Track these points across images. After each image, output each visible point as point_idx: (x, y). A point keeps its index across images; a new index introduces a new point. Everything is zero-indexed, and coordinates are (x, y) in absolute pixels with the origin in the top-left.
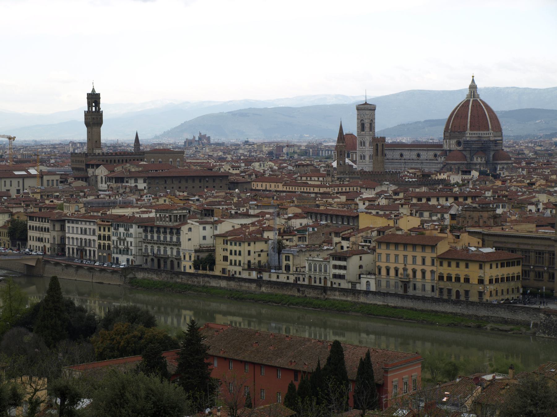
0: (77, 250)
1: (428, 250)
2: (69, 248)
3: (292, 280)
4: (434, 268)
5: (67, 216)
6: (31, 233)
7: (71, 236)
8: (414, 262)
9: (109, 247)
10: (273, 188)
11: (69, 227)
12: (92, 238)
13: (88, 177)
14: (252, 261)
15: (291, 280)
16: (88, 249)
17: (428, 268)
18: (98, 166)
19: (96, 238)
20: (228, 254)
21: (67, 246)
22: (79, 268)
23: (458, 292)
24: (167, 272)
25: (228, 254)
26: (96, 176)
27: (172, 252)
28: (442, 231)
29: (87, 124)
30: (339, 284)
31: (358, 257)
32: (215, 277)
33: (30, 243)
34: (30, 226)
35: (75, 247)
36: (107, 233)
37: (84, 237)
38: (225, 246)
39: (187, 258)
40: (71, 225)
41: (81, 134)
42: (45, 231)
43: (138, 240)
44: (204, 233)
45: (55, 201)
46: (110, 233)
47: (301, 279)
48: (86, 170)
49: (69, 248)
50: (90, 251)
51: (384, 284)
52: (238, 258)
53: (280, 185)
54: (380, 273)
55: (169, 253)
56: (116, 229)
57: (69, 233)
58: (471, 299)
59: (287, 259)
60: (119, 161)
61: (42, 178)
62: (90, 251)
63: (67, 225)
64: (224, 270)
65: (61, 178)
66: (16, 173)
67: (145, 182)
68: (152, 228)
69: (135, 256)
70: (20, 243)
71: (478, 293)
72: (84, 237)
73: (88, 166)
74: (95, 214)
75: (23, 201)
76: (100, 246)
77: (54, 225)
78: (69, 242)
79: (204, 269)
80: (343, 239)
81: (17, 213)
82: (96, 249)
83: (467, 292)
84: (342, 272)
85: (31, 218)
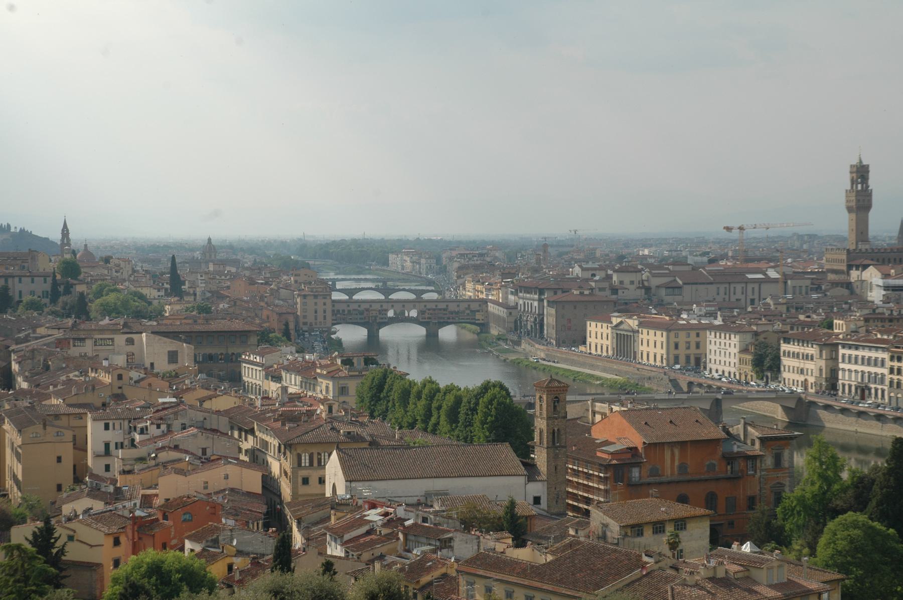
0: (856, 389)
2: (844, 385)
5: (839, 339)
6: (786, 361)
11: (844, 355)
12: (879, 370)
13: (851, 283)
16: (873, 386)
18: (865, 267)
19: (885, 371)
21: (840, 382)
22: (861, 414)
26: (863, 281)
29: (850, 210)
33: (785, 375)
34: (784, 352)
35: (853, 384)
37: (867, 369)
40: (847, 352)
41: (841, 223)
42: (807, 358)
45: (815, 316)
48: (848, 274)
49: (844, 385)
50: (876, 390)
57: (843, 361)
60: (895, 260)
61: (786, 283)
62: (876, 390)
63: (841, 351)
65: (812, 284)
66: (750, 276)
70: (769, 374)
72: (867, 369)
73: (850, 267)
75: (765, 316)
76: (891, 382)
77: (821, 351)
78: (844, 376)
81: (764, 332)
82: (886, 388)
85: (787, 341)
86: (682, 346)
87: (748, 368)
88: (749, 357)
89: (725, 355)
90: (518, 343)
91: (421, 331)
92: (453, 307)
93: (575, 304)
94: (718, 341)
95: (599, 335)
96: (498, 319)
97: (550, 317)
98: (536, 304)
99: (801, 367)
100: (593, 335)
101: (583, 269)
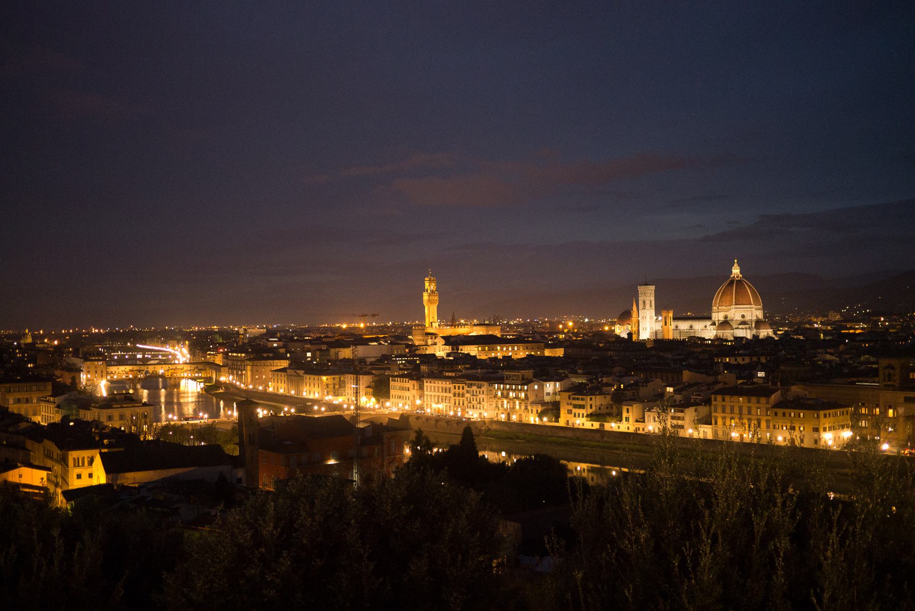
1: (763, 400)
6: (392, 392)
7: (429, 393)
8: (749, 413)
15: (632, 430)
19: (451, 395)
23: (793, 441)
27: (520, 406)
31: (693, 409)
36: (461, 391)
38: (570, 401)
39: (535, 411)
40: (429, 384)
46: (465, 391)
51: (720, 433)
52: (582, 411)
54: (716, 423)
55: (517, 407)
56: (470, 386)
58: (805, 446)
63: (425, 384)
71: (813, 441)
74: (450, 374)
83: (802, 441)
84: (680, 422)
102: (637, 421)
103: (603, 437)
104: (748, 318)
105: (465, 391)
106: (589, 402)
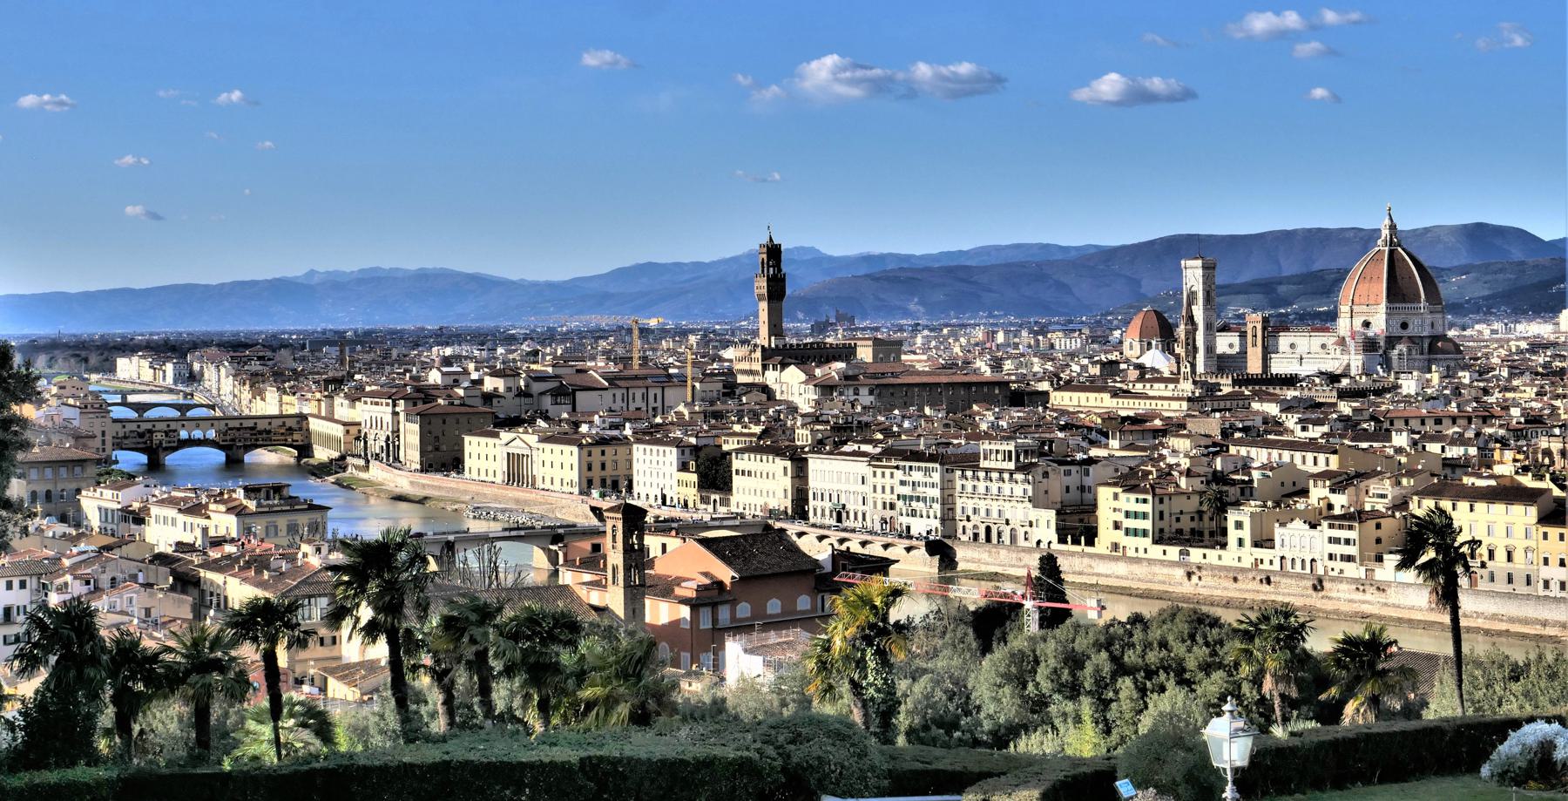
1: (1518, 509)
3: (1247, 563)
4: (1532, 544)
9: (892, 506)
10: (1092, 403)
14: (1167, 529)
17: (1519, 544)
18: (784, 366)
19: (868, 489)
20: (1120, 517)
24: (1008, 548)
25: (1120, 517)
28: (1541, 478)
30: (1342, 571)
32: (1101, 557)
43: (947, 492)
44: (1067, 480)
47: (1266, 562)
53: (1106, 396)
59: (1239, 525)
64: (1115, 546)
67: (871, 393)
68: (976, 468)
69: (943, 520)
73: (765, 367)
79: (1076, 542)
80: (1333, 491)
86: (596, 466)
87: (692, 494)
88: (694, 478)
89: (658, 475)
90: (366, 468)
91: (219, 457)
92: (262, 425)
93: (443, 416)
94: (648, 457)
95: (484, 455)
96: (328, 441)
97: (411, 434)
98: (388, 418)
99: (759, 486)
100: (475, 456)
101: (444, 374)
102: (1256, 544)
103: (1189, 575)
104: (1413, 330)
105: (896, 481)
106: (1160, 507)
